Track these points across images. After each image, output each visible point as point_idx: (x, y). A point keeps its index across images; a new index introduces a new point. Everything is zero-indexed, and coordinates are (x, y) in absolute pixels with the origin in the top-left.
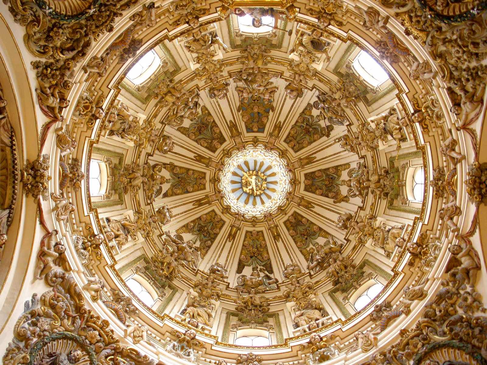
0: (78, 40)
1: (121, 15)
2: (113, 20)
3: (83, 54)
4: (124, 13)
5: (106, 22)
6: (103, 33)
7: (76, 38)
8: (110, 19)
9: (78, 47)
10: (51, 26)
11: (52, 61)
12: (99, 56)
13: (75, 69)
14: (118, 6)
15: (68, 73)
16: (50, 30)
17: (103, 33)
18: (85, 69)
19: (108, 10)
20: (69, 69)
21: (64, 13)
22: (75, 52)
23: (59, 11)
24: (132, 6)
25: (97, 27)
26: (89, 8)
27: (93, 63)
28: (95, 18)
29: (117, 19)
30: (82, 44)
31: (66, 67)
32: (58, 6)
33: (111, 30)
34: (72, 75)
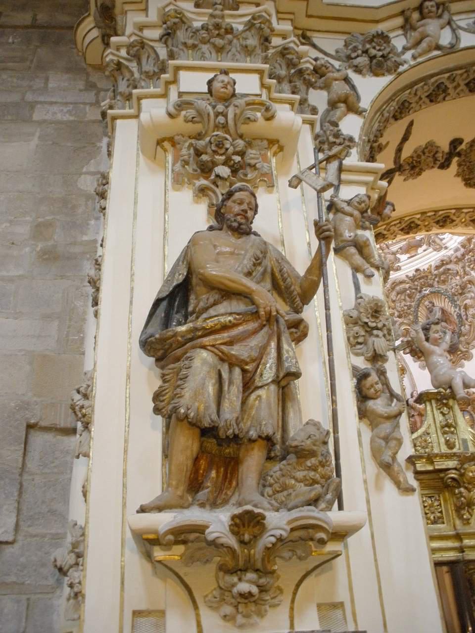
0: (444, 273)
1: (407, 276)
2: (414, 276)
3: (443, 263)
4: (404, 277)
5: (420, 279)
6: (424, 270)
7: (445, 276)
8: (415, 278)
9: (445, 270)
10: (459, 296)
11: (467, 269)
12: (431, 250)
13: (453, 253)
14: (407, 286)
15: (459, 254)
16: (461, 294)
17: (424, 270)
18: (446, 248)
19: (414, 285)
20: (457, 257)
21: (446, 300)
22: (448, 266)
23: (450, 303)
24: (398, 281)
25: (427, 276)
26: (428, 295)
27: (438, 247)
28: (426, 285)
29: (411, 275)
30: (441, 270)
31: (459, 260)
32: (449, 307)
33: (417, 270)
34: (457, 250)
